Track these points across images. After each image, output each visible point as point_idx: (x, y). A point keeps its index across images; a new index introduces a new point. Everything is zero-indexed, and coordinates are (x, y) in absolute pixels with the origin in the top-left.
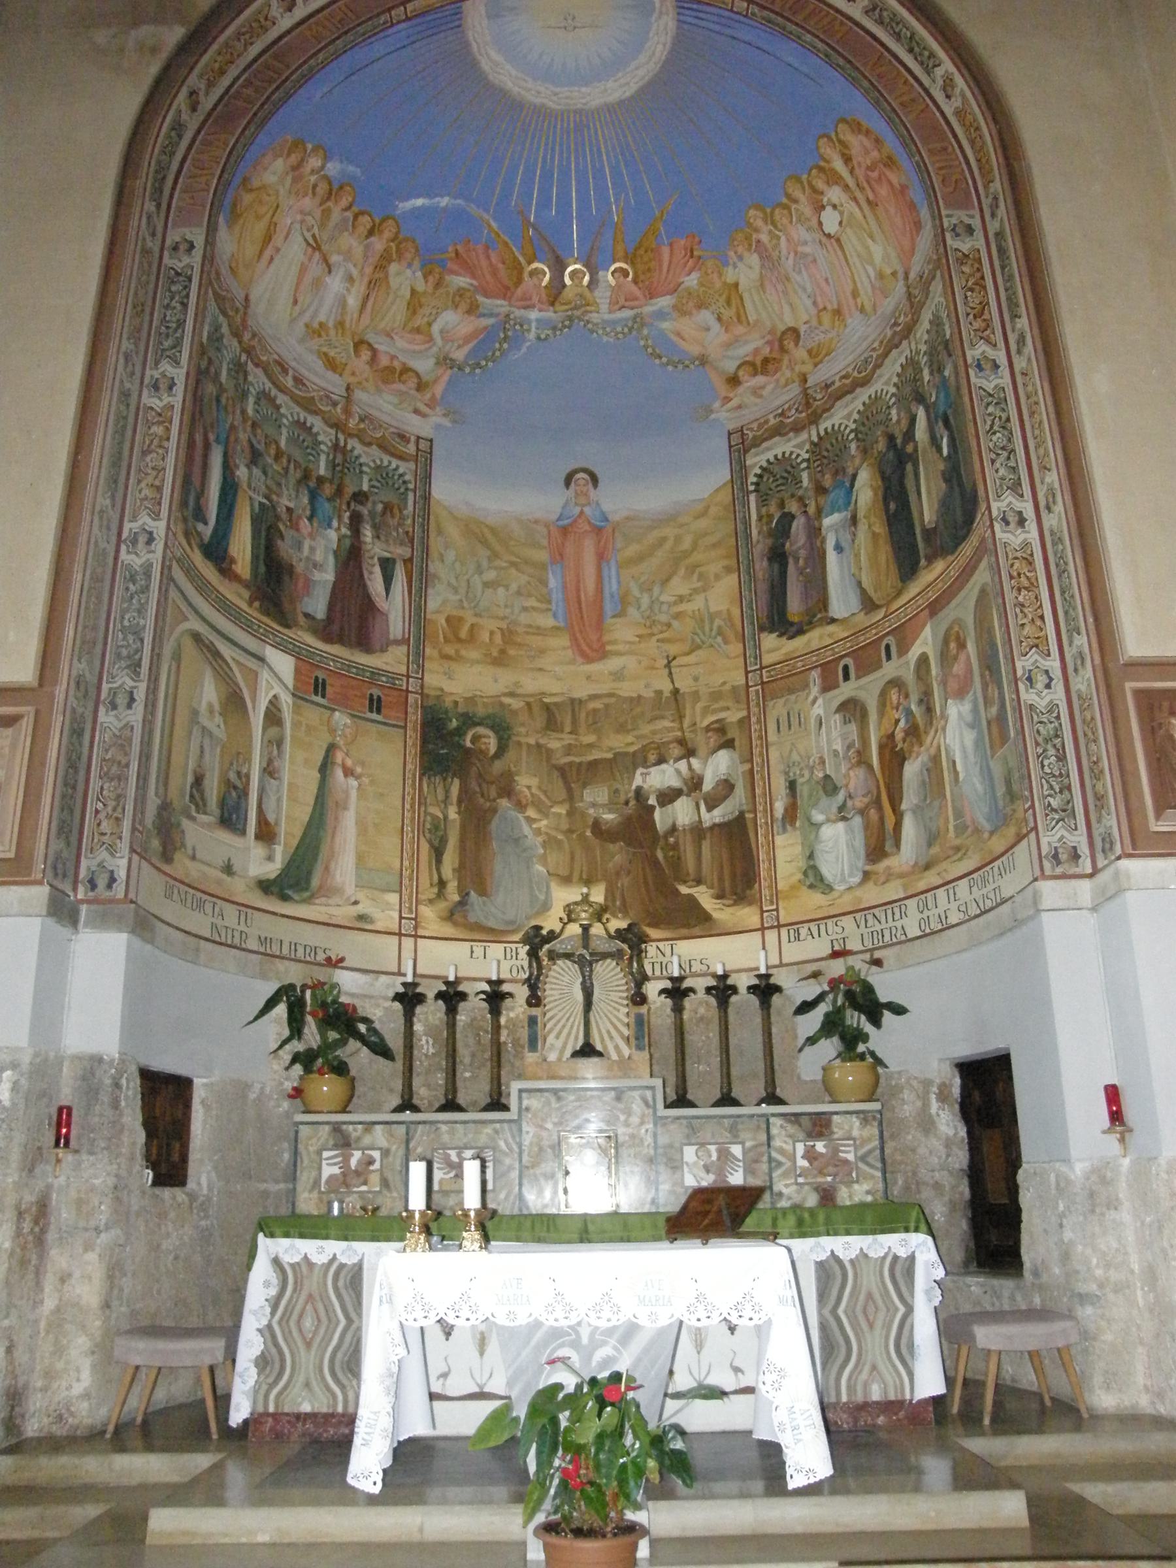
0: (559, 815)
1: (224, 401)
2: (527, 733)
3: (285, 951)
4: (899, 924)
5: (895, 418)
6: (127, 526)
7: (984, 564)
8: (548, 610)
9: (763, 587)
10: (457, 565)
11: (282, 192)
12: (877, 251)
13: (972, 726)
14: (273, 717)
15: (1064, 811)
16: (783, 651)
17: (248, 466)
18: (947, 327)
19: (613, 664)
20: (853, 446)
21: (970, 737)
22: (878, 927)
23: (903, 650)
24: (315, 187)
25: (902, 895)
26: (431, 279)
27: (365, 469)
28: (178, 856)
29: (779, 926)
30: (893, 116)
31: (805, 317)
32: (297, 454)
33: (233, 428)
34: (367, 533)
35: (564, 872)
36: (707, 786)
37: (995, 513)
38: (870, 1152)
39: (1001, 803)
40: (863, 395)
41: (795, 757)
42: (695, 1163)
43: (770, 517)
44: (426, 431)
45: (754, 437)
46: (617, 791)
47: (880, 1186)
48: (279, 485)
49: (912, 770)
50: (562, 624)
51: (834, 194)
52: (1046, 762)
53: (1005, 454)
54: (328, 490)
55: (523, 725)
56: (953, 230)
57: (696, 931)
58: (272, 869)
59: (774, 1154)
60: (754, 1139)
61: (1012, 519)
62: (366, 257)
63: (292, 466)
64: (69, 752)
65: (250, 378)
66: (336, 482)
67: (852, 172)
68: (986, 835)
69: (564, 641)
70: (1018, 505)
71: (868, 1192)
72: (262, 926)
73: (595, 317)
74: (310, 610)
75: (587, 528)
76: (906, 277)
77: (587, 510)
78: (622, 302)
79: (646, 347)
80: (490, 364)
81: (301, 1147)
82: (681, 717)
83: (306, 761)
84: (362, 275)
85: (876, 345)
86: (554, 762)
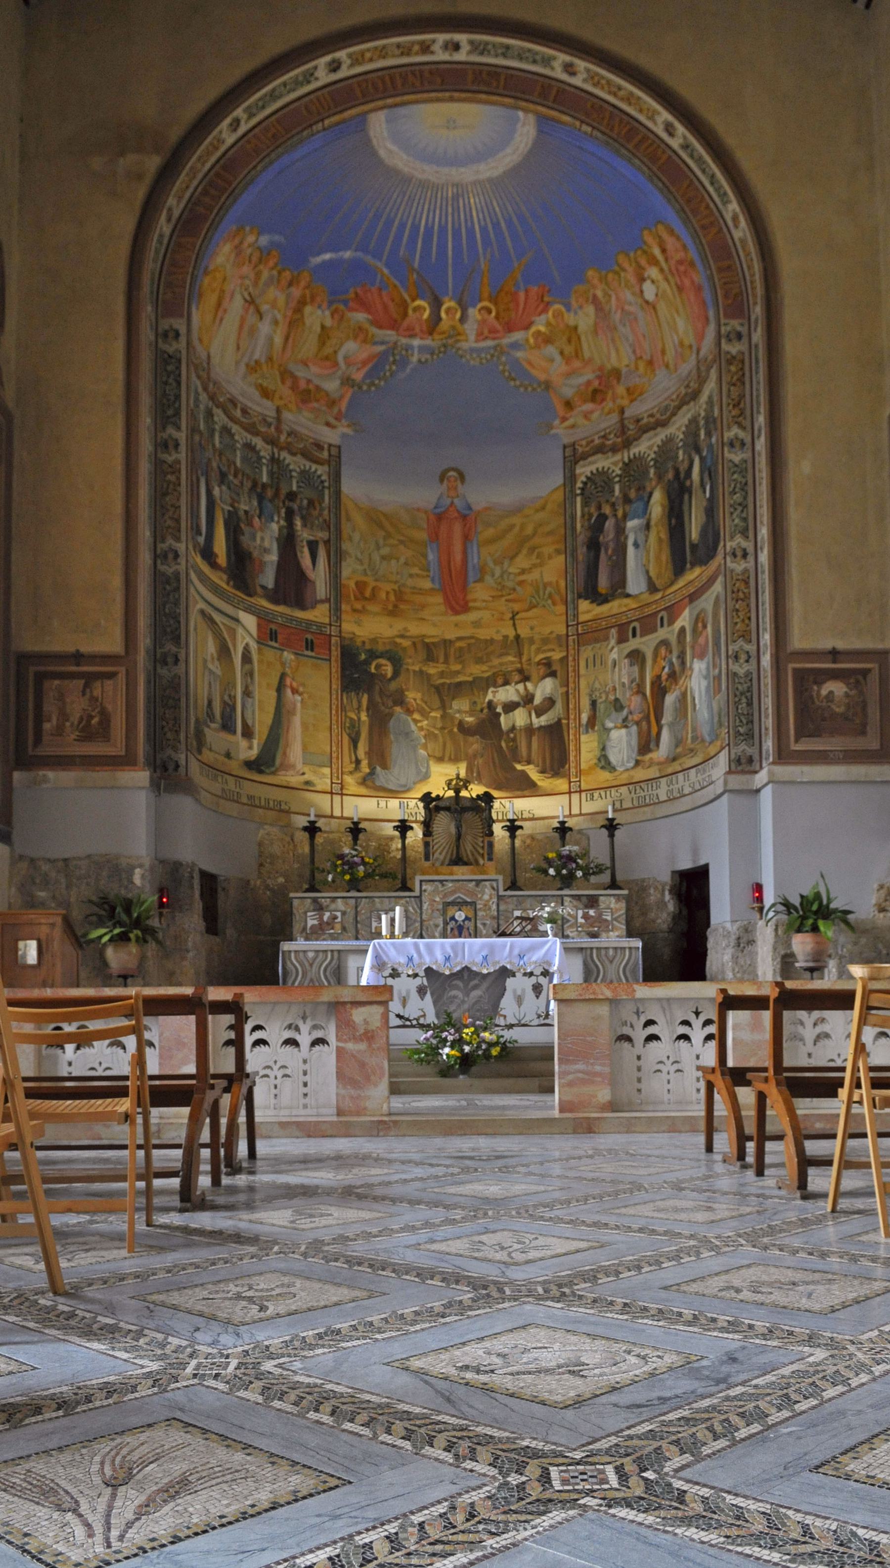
10: (362, 545)
14: (247, 658)
19: (472, 616)
28: (204, 750)
34: (298, 523)
41: (597, 685)
49: (670, 699)
50: (437, 586)
69: (439, 599)
74: (264, 583)
75: (456, 515)
77: (456, 501)
80: (382, 383)
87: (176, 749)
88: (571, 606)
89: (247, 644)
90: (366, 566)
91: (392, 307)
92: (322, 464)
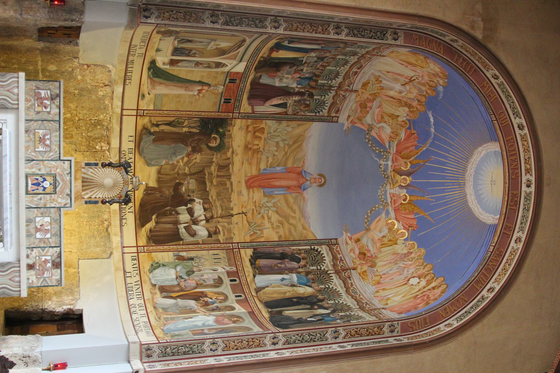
0: (185, 170)
1: (339, 49)
2: (217, 158)
3: (129, 69)
4: (135, 297)
5: (329, 302)
6: (282, 19)
7: (261, 330)
8: (267, 167)
9: (271, 250)
10: (285, 132)
11: (428, 69)
12: (398, 298)
13: (203, 325)
14: (218, 65)
15: (165, 353)
16: (245, 257)
17: (316, 56)
18: (355, 321)
20: (323, 286)
21: (200, 324)
22: (134, 289)
23: (238, 302)
24: (433, 81)
25: (145, 298)
26: (403, 123)
27: (323, 97)
28: (160, 36)
29: (138, 253)
30: (442, 305)
31: (379, 270)
32: (325, 73)
33: (330, 52)
34: (297, 98)
35: (163, 171)
36: (194, 227)
37: (277, 334)
38: (47, 283)
39: (171, 333)
40: (341, 290)
41: (202, 260)
42: (44, 221)
43: (300, 254)
44: (341, 120)
45: (334, 249)
46: (194, 192)
47: (35, 285)
48: (312, 67)
49: (192, 303)
50: (261, 172)
51: (423, 283)
52: (183, 348)
53: (301, 339)
54: (313, 84)
55: (221, 156)
56: (392, 325)
57: (138, 221)
58: (160, 64)
59: (47, 249)
60: (52, 242)
61: (275, 340)
62: (409, 99)
63: (320, 71)
64: (193, 3)
65: (352, 57)
66: (317, 87)
67: (429, 290)
68: (162, 328)
69: (254, 172)
70: (280, 343)
71: (33, 281)
72: (138, 62)
73: (388, 187)
75: (300, 183)
76: (383, 308)
77: (308, 182)
78: (394, 198)
79: (375, 207)
80: (370, 145)
81: (51, 83)
82: (222, 217)
83: (203, 76)
84: (403, 97)
85: (361, 297)
86: (205, 168)
87: (158, 17)
88: (249, 245)
89: (227, 65)
90: (273, 134)
91: (407, 151)
92: (328, 113)
